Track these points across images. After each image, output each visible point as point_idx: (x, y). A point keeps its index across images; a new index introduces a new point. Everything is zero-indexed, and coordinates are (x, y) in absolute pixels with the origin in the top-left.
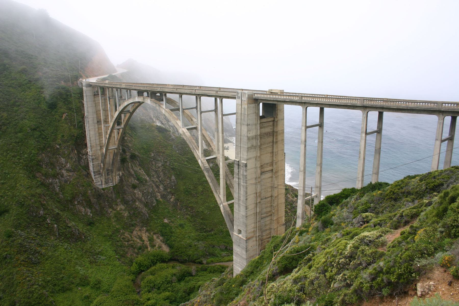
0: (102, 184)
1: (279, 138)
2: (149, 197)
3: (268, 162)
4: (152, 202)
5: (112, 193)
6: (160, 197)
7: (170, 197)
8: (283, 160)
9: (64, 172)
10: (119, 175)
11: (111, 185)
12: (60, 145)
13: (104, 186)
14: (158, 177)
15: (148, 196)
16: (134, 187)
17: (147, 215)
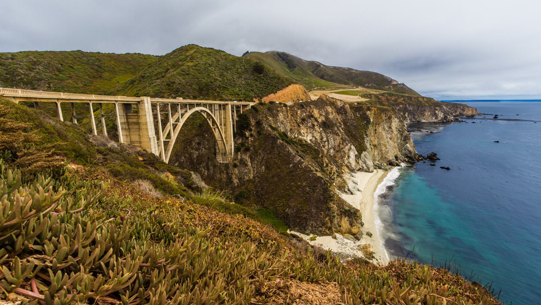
0: (220, 161)
1: (143, 127)
2: (242, 175)
3: (138, 140)
4: (244, 179)
5: (223, 166)
6: (252, 177)
7: (256, 179)
8: (148, 142)
9: (204, 149)
10: (231, 157)
11: (225, 162)
12: (208, 135)
13: (221, 162)
14: (257, 165)
15: (241, 174)
16: (235, 166)
17: (236, 185)
